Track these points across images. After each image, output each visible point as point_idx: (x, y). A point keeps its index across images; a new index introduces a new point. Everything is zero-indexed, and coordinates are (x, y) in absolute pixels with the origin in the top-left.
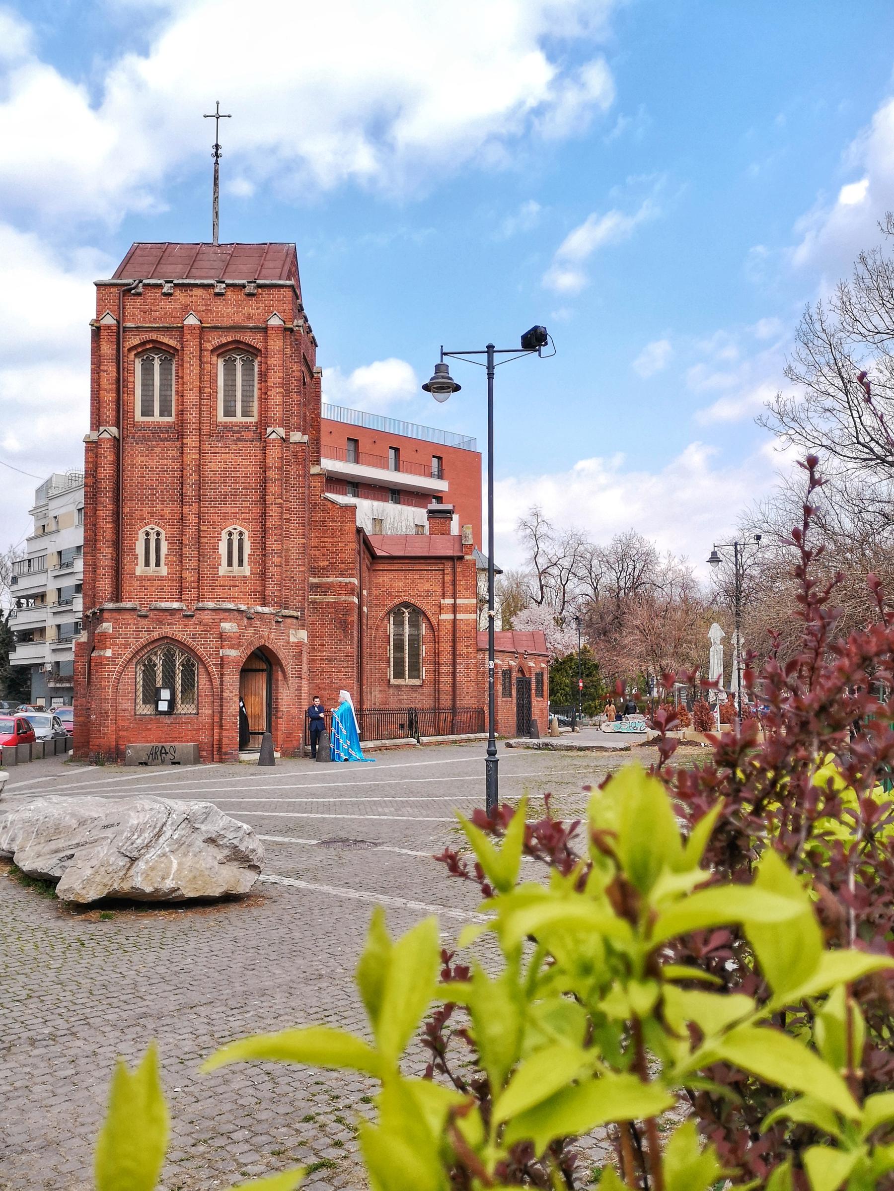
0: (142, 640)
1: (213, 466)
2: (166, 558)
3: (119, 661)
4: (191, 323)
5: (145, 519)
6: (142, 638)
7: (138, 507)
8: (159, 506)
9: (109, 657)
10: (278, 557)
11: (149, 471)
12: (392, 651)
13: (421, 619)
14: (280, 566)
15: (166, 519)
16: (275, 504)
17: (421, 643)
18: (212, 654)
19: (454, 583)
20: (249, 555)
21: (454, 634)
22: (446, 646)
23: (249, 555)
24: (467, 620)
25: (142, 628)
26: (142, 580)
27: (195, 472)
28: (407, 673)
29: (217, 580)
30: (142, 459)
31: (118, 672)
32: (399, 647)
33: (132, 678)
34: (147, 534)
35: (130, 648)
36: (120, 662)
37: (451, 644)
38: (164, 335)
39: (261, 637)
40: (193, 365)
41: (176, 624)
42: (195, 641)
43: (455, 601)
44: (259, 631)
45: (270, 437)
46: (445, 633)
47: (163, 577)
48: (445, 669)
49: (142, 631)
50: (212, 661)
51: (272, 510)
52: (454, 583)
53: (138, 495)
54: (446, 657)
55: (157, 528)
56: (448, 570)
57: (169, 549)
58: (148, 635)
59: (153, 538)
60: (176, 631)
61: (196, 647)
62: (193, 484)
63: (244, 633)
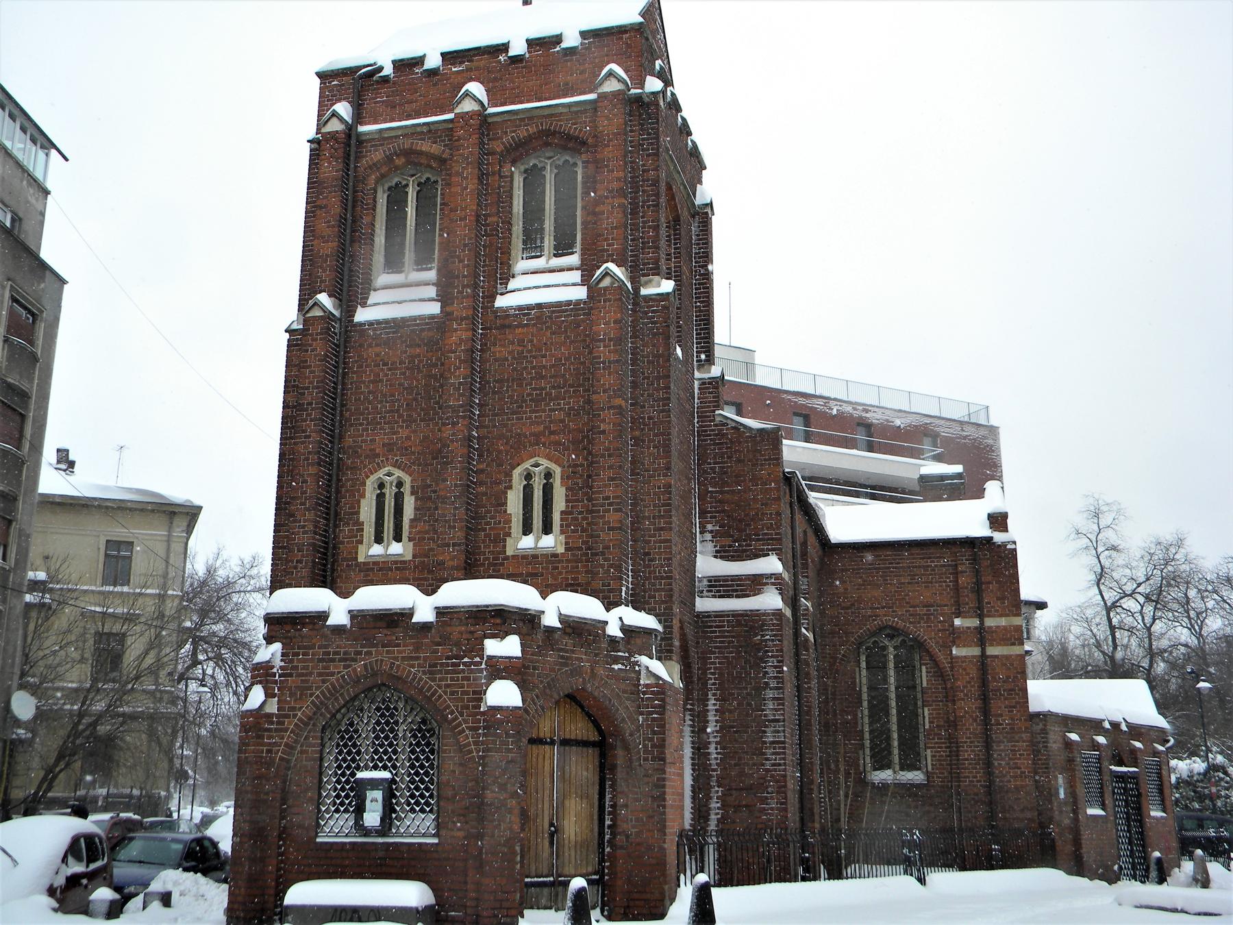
0: (333, 679)
1: (499, 351)
2: (411, 527)
3: (290, 723)
4: (466, 110)
5: (378, 456)
6: (332, 674)
7: (368, 435)
8: (403, 433)
9: (270, 716)
10: (616, 510)
11: (390, 369)
12: (866, 720)
13: (917, 657)
14: (620, 528)
15: (413, 453)
16: (609, 408)
17: (920, 703)
18: (467, 707)
19: (978, 590)
20: (562, 512)
21: (984, 683)
22: (968, 706)
23: (562, 512)
24: (1007, 657)
25: (336, 653)
26: (368, 570)
27: (465, 361)
28: (896, 759)
29: (502, 564)
30: (377, 350)
31: (286, 745)
32: (879, 708)
33: (314, 759)
34: (381, 486)
35: (311, 695)
36: (290, 724)
37: (979, 703)
38: (424, 140)
39: (577, 672)
40: (467, 178)
41: (398, 645)
42: (434, 680)
43: (982, 623)
44: (567, 658)
45: (601, 285)
46: (966, 682)
47: (405, 562)
48: (970, 752)
49: (333, 660)
50: (466, 722)
51: (604, 421)
52: (978, 590)
53: (369, 414)
54: (970, 729)
55: (398, 473)
56: (965, 566)
57: (416, 509)
58: (345, 667)
59: (390, 492)
60: (396, 659)
61: (436, 691)
62: (460, 383)
63: (538, 661)
